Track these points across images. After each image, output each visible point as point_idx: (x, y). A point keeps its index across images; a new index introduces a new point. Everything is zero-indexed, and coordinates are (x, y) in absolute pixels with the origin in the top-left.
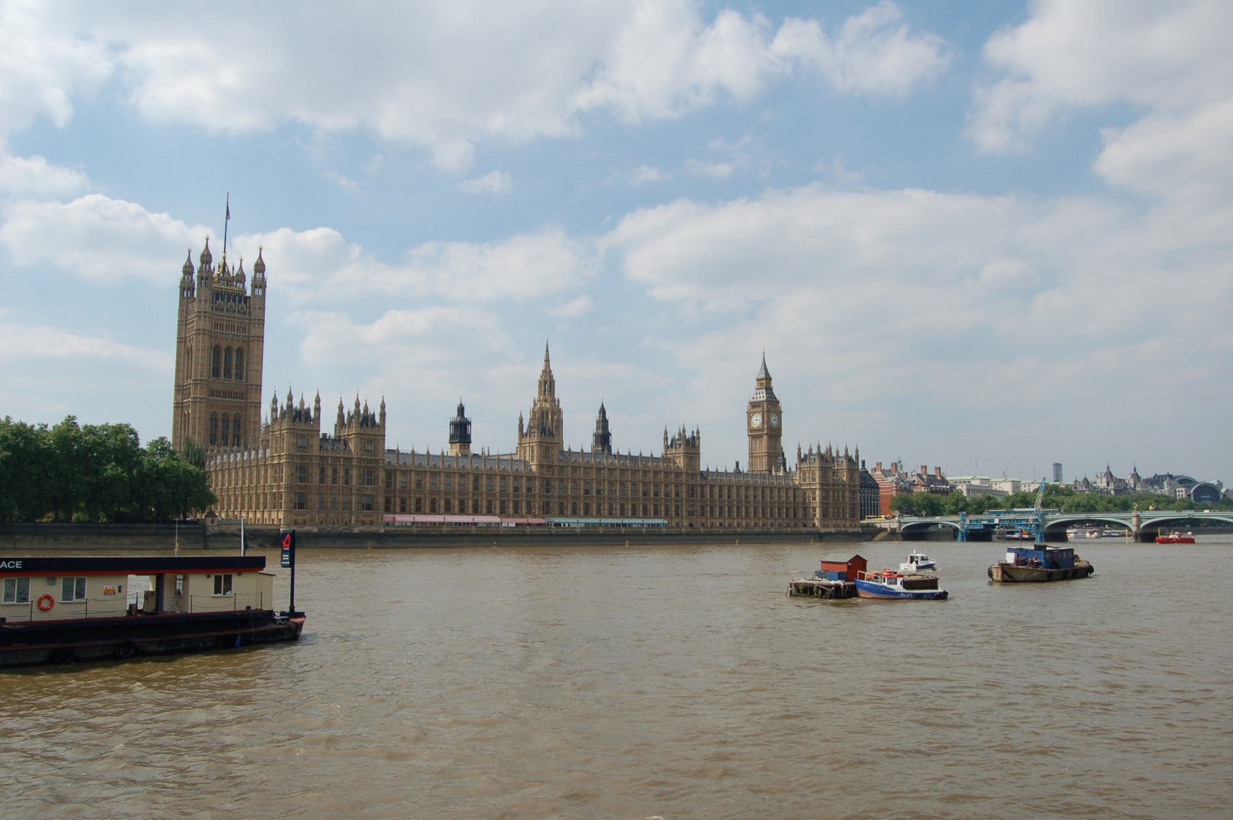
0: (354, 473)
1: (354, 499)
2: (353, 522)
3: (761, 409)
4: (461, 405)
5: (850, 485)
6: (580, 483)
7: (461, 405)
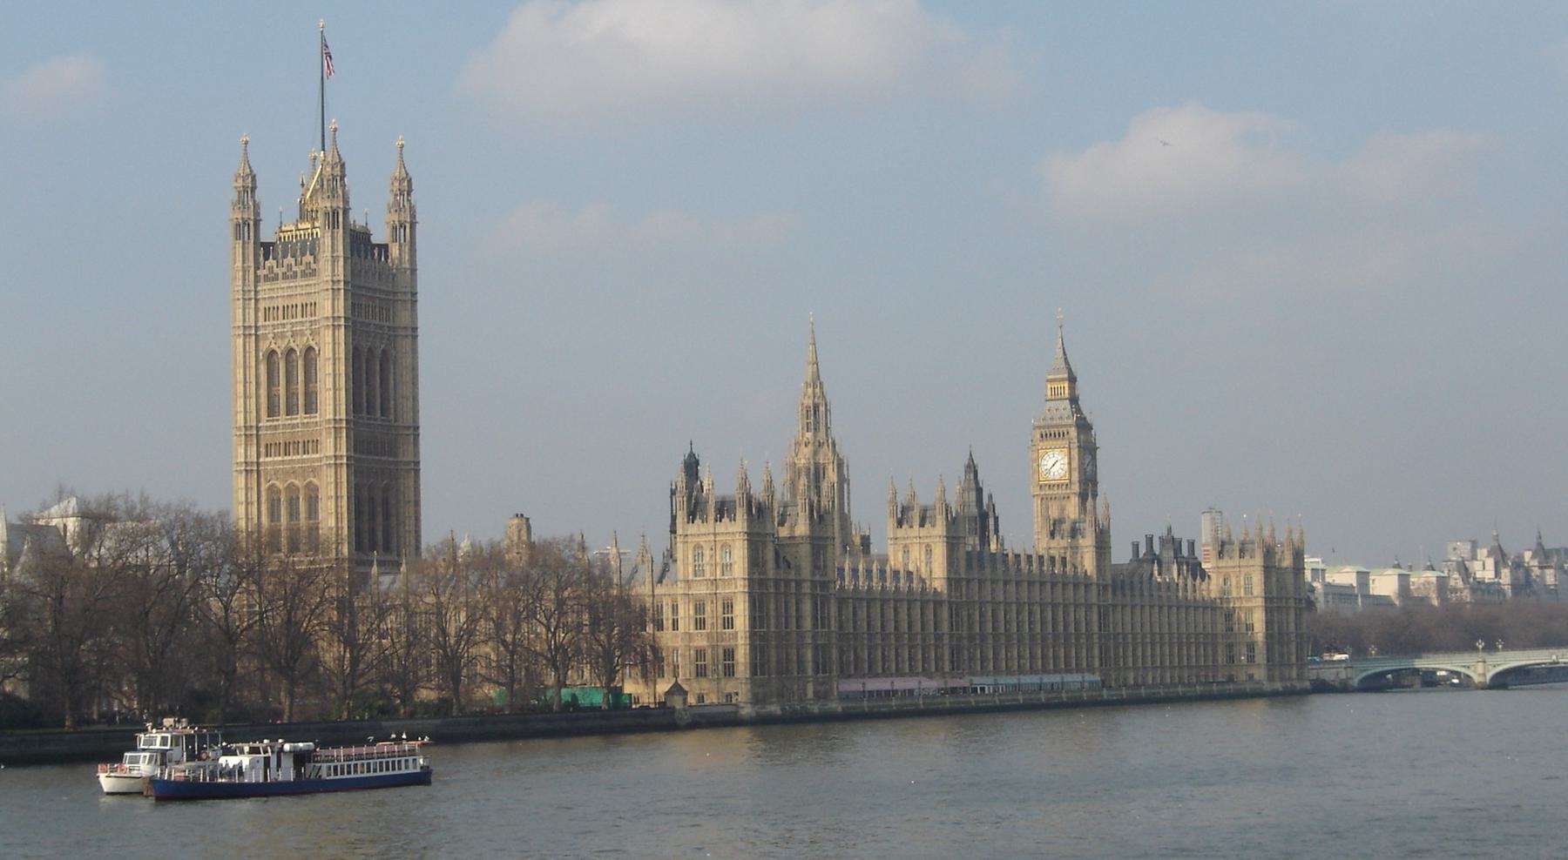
0: (807, 607)
1: (809, 654)
2: (810, 694)
3: (1065, 443)
4: (692, 455)
5: (1295, 599)
6: (986, 608)
7: (692, 455)
